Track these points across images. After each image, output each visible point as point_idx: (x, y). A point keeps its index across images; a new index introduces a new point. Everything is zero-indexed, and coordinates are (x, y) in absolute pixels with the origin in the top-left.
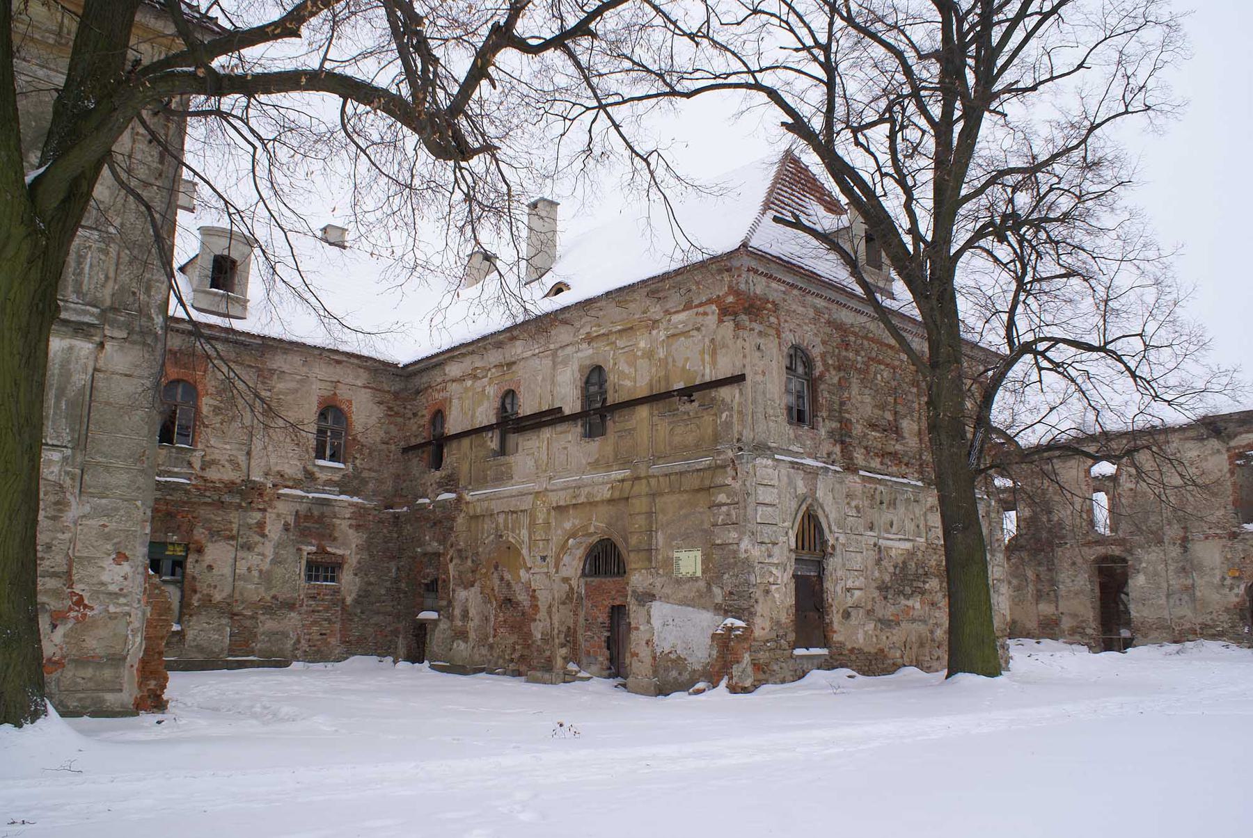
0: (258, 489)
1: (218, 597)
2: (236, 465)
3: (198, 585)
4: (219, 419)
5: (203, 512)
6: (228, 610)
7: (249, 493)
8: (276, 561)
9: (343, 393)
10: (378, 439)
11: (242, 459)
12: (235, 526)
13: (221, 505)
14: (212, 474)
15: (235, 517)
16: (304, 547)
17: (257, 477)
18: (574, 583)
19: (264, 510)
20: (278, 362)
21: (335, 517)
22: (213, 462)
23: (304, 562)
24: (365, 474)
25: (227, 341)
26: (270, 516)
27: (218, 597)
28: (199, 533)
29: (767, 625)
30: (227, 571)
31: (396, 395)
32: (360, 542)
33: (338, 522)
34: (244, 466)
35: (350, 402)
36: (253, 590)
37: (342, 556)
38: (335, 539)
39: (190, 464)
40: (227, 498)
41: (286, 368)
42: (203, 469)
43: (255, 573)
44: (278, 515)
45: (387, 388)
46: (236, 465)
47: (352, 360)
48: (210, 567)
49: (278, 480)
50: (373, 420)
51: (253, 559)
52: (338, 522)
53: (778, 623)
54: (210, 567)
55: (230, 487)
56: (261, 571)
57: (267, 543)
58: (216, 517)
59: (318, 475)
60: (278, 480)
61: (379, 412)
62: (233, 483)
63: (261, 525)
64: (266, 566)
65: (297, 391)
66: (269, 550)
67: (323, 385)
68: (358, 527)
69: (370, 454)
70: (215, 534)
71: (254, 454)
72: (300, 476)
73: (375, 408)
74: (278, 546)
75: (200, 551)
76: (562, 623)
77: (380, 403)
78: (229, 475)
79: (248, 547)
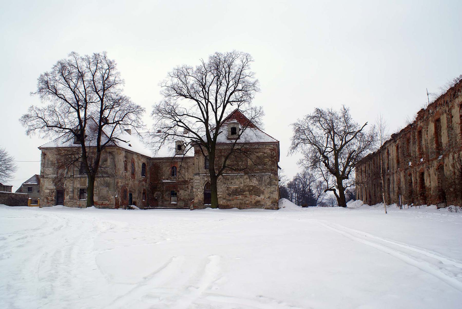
0: (187, 181)
2: (183, 178)
6: (183, 200)
14: (180, 180)
15: (184, 186)
20: (188, 160)
26: (189, 185)
28: (178, 189)
29: (197, 201)
36: (187, 197)
46: (183, 178)
51: (187, 192)
53: (200, 200)
55: (183, 181)
58: (181, 186)
63: (188, 187)
66: (189, 191)
70: (181, 189)
75: (179, 191)
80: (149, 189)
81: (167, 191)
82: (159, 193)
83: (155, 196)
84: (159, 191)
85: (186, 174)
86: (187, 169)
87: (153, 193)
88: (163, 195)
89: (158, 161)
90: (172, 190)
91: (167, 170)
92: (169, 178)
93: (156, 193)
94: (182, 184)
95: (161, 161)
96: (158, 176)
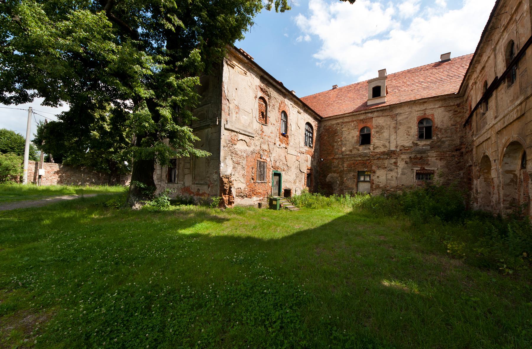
0: (393, 152)
1: (381, 186)
2: (385, 146)
3: (375, 182)
4: (378, 134)
5: (375, 161)
7: (390, 154)
8: (403, 174)
9: (429, 112)
10: (450, 125)
11: (387, 144)
12: (386, 165)
13: (379, 159)
14: (377, 150)
15: (386, 162)
16: (414, 168)
17: (393, 148)
18: (517, 173)
19: (397, 158)
20: (398, 111)
21: (428, 157)
22: (377, 147)
23: (415, 174)
24: (444, 139)
25: (378, 111)
26: (399, 161)
27: (381, 186)
28: (374, 168)
30: (384, 177)
31: (458, 105)
32: (442, 164)
33: (429, 158)
34: (388, 146)
35: (433, 115)
37: (433, 170)
38: (429, 165)
39: (369, 149)
40: (382, 157)
41: (401, 112)
42: (374, 150)
43: (395, 178)
44: (402, 159)
45: (452, 104)
47: (430, 100)
48: (378, 177)
49: (402, 148)
50: (446, 118)
51: (393, 174)
52: (429, 158)
54: (378, 177)
55: (383, 153)
56: (396, 177)
57: (399, 169)
58: (380, 162)
59: (419, 144)
60: (402, 148)
61: (448, 115)
62: (384, 152)
63: (395, 163)
64: (399, 176)
65: (407, 117)
66: (400, 171)
67: (419, 113)
68: (441, 159)
69: (445, 131)
70: (379, 167)
71: (391, 142)
72: (411, 145)
73: (447, 113)
74: (403, 169)
75: (374, 172)
76: (505, 195)
77: (451, 111)
78: (382, 149)
79: (391, 170)
80: (318, 169)
81: (349, 171)
82: (335, 175)
83: (327, 180)
84: (335, 172)
85: (393, 137)
86: (395, 128)
87: (325, 176)
88: (342, 177)
89: (334, 122)
90: (362, 170)
91: (350, 135)
92: (354, 148)
93: (330, 175)
94: (383, 159)
95: (339, 121)
96: (333, 146)
